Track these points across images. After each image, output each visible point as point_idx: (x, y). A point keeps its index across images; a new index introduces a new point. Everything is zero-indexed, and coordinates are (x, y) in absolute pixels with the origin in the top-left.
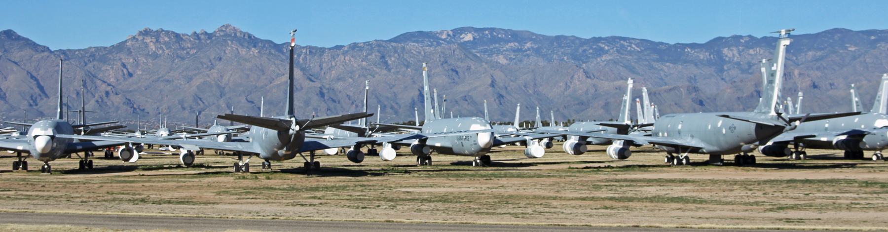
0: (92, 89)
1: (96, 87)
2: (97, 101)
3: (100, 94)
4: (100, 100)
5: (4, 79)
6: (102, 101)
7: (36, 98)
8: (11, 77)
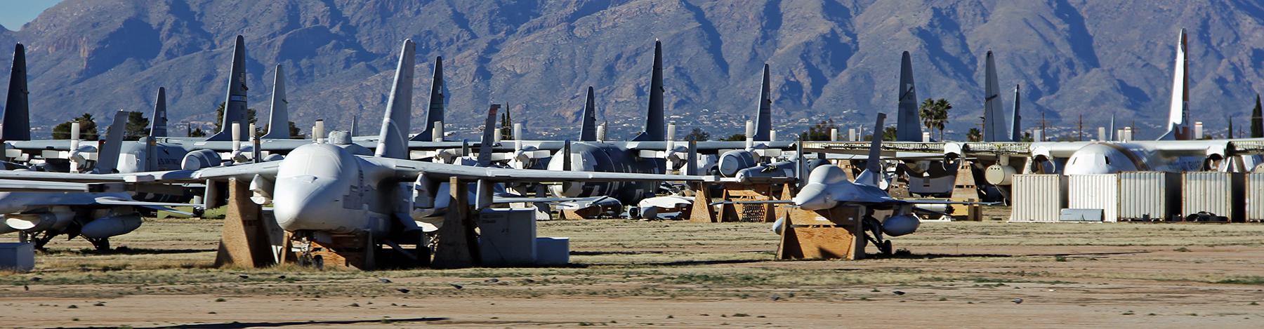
0: (1225, 44)
1: (1237, 38)
2: (1221, 81)
3: (1235, 59)
4: (1231, 78)
5: (979, 17)
6: (1237, 80)
7: (1058, 71)
8: (999, 14)
